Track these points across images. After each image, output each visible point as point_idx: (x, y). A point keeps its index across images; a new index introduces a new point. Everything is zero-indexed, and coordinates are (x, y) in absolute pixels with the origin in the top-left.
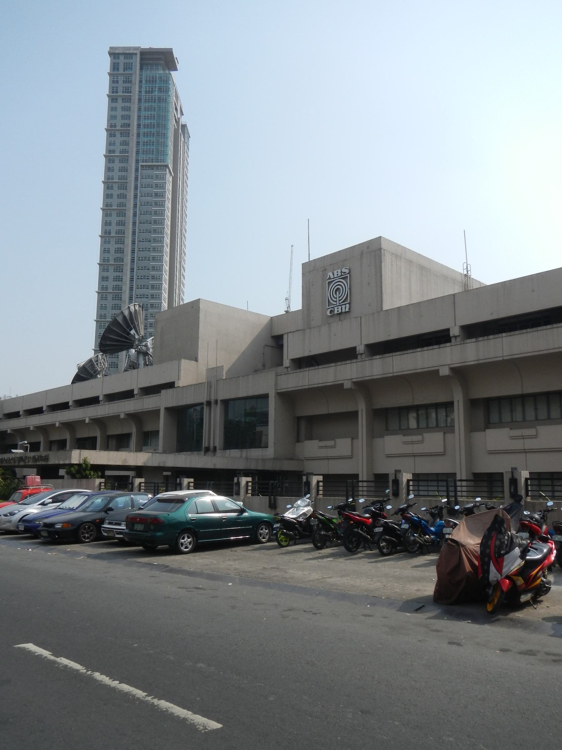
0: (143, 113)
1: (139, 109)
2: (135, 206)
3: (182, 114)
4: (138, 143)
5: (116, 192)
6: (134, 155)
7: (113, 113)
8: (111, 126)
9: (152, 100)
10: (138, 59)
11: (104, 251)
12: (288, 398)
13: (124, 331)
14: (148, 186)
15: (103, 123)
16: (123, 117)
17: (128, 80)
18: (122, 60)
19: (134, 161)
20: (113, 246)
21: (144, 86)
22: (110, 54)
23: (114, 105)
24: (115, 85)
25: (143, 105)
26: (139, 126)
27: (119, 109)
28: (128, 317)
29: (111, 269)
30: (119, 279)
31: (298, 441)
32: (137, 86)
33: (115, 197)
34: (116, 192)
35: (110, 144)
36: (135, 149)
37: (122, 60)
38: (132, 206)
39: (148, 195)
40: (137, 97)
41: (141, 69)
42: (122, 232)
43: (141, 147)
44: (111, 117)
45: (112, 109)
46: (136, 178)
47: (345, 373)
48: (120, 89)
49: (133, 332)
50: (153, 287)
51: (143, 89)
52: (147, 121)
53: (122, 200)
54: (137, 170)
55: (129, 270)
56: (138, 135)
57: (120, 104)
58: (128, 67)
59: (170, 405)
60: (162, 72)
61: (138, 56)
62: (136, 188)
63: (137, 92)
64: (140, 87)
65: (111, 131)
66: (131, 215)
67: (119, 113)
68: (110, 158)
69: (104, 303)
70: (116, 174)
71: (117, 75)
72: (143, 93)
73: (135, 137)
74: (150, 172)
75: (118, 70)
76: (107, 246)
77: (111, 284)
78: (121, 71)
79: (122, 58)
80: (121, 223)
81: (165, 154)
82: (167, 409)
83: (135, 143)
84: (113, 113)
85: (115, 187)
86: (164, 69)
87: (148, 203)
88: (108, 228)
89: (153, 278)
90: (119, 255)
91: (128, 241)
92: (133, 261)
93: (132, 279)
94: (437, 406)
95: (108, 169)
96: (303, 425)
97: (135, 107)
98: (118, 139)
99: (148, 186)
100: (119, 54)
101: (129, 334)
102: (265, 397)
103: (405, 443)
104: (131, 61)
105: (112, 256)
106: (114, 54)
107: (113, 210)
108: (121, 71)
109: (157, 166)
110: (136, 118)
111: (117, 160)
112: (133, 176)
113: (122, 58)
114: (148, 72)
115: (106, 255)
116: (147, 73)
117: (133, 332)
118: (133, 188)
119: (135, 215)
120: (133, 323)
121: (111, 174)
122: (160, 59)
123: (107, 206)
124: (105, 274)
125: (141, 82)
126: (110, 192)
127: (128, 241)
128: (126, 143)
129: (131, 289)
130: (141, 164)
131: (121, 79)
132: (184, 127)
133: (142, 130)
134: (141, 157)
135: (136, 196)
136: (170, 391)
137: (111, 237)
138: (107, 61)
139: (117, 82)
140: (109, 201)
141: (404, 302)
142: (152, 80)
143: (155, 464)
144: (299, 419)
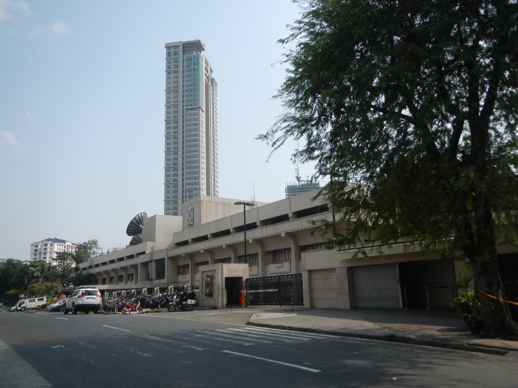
0: (185, 79)
1: (183, 77)
2: (183, 132)
3: (211, 71)
4: (183, 96)
5: (172, 125)
6: (181, 103)
7: (169, 81)
8: (168, 88)
9: (190, 71)
10: (181, 48)
11: (167, 160)
12: (174, 259)
13: (137, 226)
14: (190, 120)
15: (164, 87)
16: (174, 82)
17: (176, 61)
18: (173, 50)
19: (181, 106)
20: (172, 157)
21: (185, 63)
22: (166, 47)
23: (169, 76)
24: (169, 64)
25: (185, 74)
26: (183, 86)
27: (172, 78)
28: (138, 220)
29: (171, 170)
30: (176, 175)
31: (179, 275)
32: (181, 64)
33: (172, 128)
34: (172, 125)
35: (168, 98)
36: (181, 100)
37: (173, 50)
38: (181, 132)
39: (190, 125)
40: (181, 70)
41: (184, 53)
42: (176, 148)
43: (185, 98)
44: (168, 83)
45: (168, 78)
46: (183, 116)
47: (252, 235)
48: (172, 67)
49: (141, 226)
50: (195, 178)
51: (185, 65)
52: (187, 83)
53: (176, 130)
54: (183, 111)
55: (181, 169)
56: (183, 91)
57: (172, 75)
58: (176, 53)
59: (141, 262)
60: (195, 54)
61: (181, 46)
62: (183, 122)
63: (181, 67)
64: (183, 64)
65: (168, 91)
66: (181, 138)
67: (172, 80)
68: (168, 107)
69: (168, 189)
70: (172, 115)
71: (170, 59)
72: (185, 67)
73: (181, 93)
74: (191, 112)
75: (170, 55)
76: (168, 157)
77: (172, 178)
78: (172, 56)
79: (172, 49)
80: (176, 143)
81: (198, 100)
82: (141, 263)
83: (181, 97)
84: (169, 81)
85: (172, 122)
86: (197, 52)
87: (190, 130)
88: (169, 146)
89: (195, 173)
90: (175, 161)
91: (180, 153)
92: (183, 164)
93: (183, 175)
94: (285, 250)
95: (168, 113)
96: (180, 268)
97: (181, 76)
98: (172, 95)
99: (190, 120)
100: (170, 47)
101: (139, 227)
102: (164, 258)
103: (276, 267)
104: (177, 50)
105: (172, 162)
106: (168, 47)
107: (171, 136)
108: (172, 56)
109: (194, 108)
110: (181, 81)
111: (172, 107)
112: (181, 115)
113: (172, 49)
114: (187, 55)
115: (168, 162)
116: (187, 56)
117: (141, 226)
118: (181, 122)
119: (183, 137)
120: (140, 221)
121: (169, 115)
122: (194, 46)
123: (168, 134)
124: (168, 173)
125: (183, 61)
126: (169, 126)
127: (180, 153)
128: (176, 97)
129: (183, 180)
130: (185, 108)
131: (172, 61)
132: (213, 80)
133: (185, 88)
134: (185, 104)
135: (183, 127)
136: (143, 255)
137: (171, 151)
138: (164, 51)
139: (170, 63)
140: (169, 131)
141: (213, 219)
142: (190, 59)
143: (111, 288)
144: (179, 267)
